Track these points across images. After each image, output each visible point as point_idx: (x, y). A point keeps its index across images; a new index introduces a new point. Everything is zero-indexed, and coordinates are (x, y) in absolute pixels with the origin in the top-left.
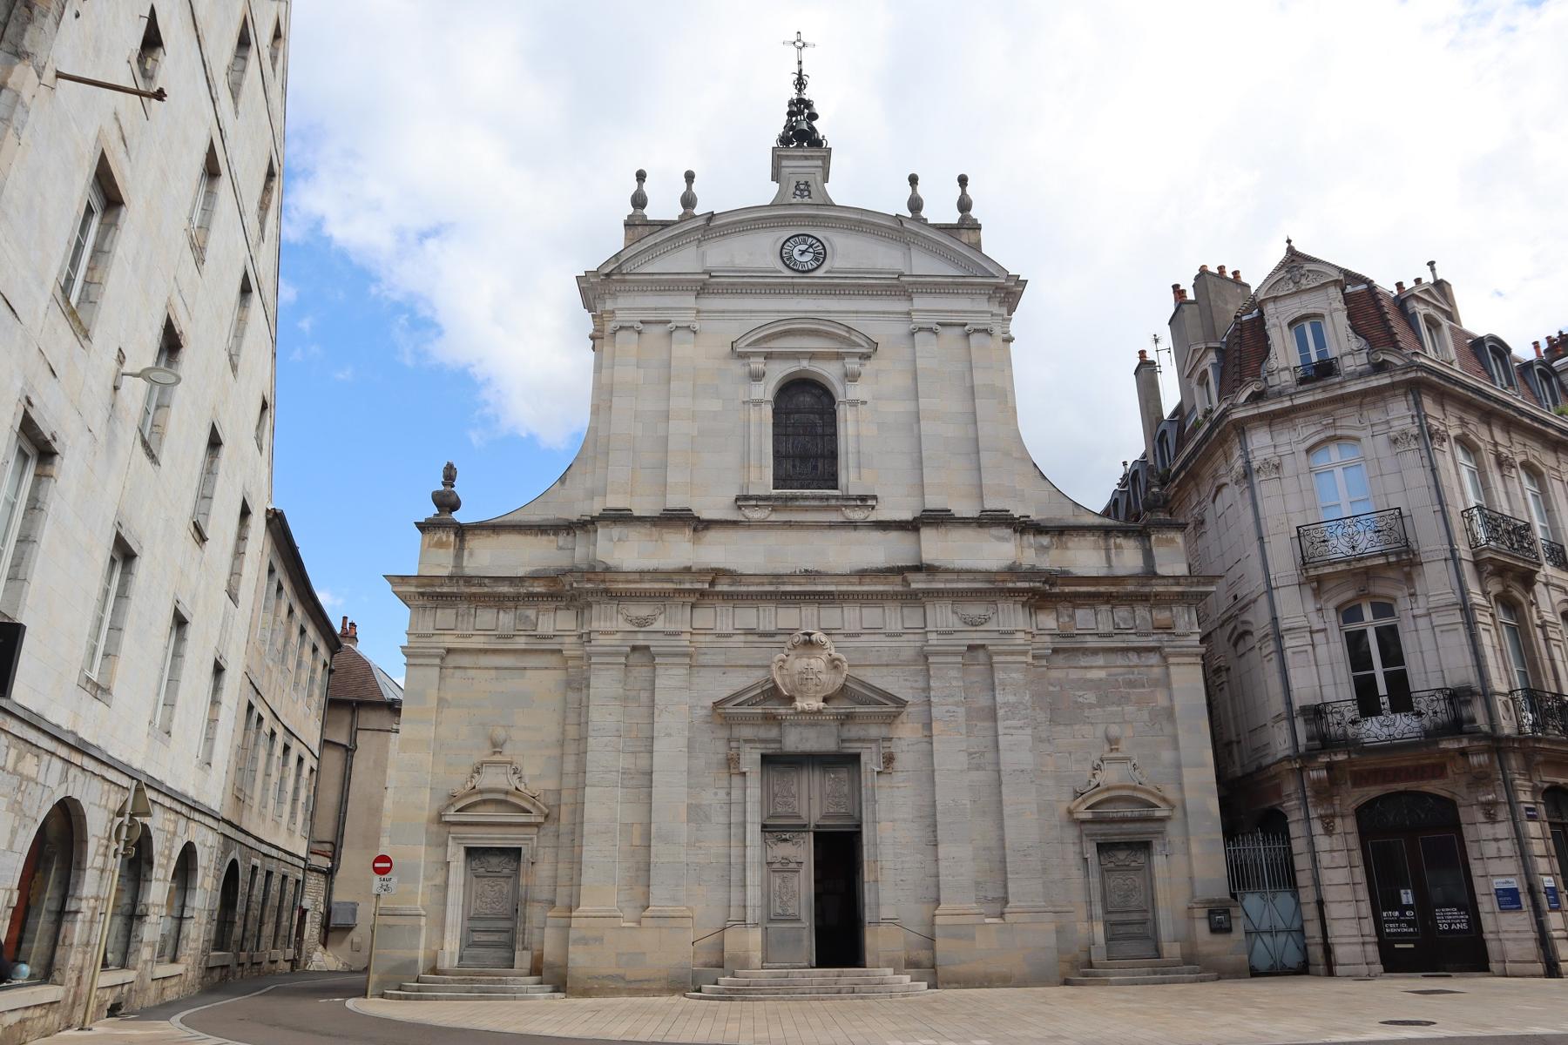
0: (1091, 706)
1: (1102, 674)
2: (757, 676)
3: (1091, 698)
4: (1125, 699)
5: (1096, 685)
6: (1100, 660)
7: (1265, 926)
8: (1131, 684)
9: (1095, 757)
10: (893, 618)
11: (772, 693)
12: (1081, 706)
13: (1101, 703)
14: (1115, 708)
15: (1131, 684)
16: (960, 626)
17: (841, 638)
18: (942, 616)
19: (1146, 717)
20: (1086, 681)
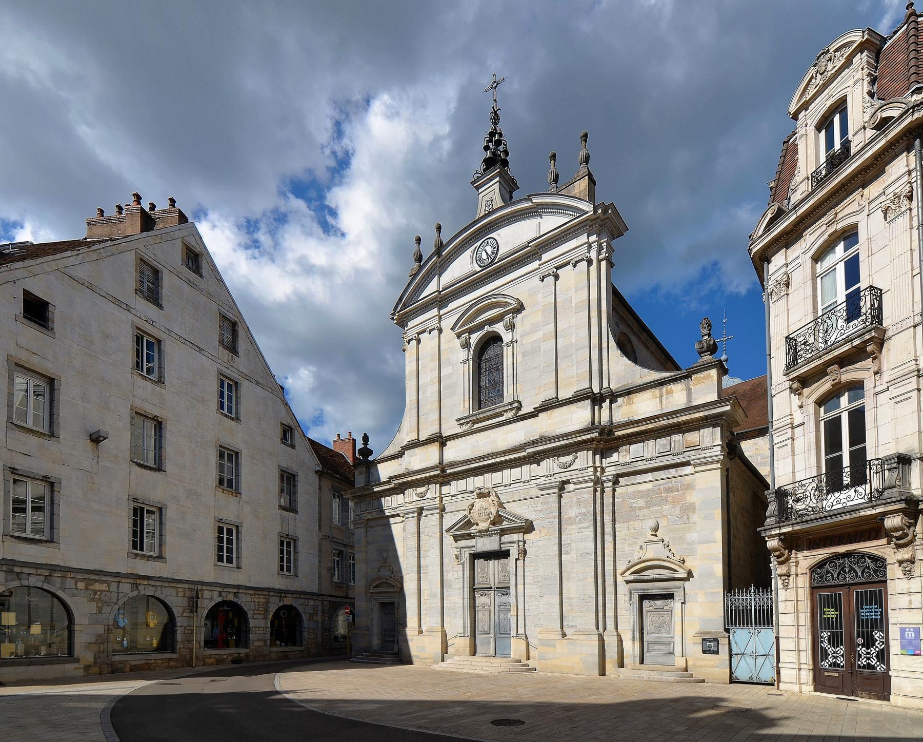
0: (640, 508)
1: (650, 486)
2: (460, 515)
3: (641, 503)
4: (666, 501)
5: (646, 494)
6: (649, 476)
7: (749, 651)
8: (669, 490)
9: (640, 542)
10: (527, 471)
11: (469, 524)
12: (633, 509)
13: (648, 506)
14: (657, 508)
15: (669, 490)
16: (557, 470)
17: (502, 488)
18: (548, 465)
19: (678, 512)
20: (639, 492)
